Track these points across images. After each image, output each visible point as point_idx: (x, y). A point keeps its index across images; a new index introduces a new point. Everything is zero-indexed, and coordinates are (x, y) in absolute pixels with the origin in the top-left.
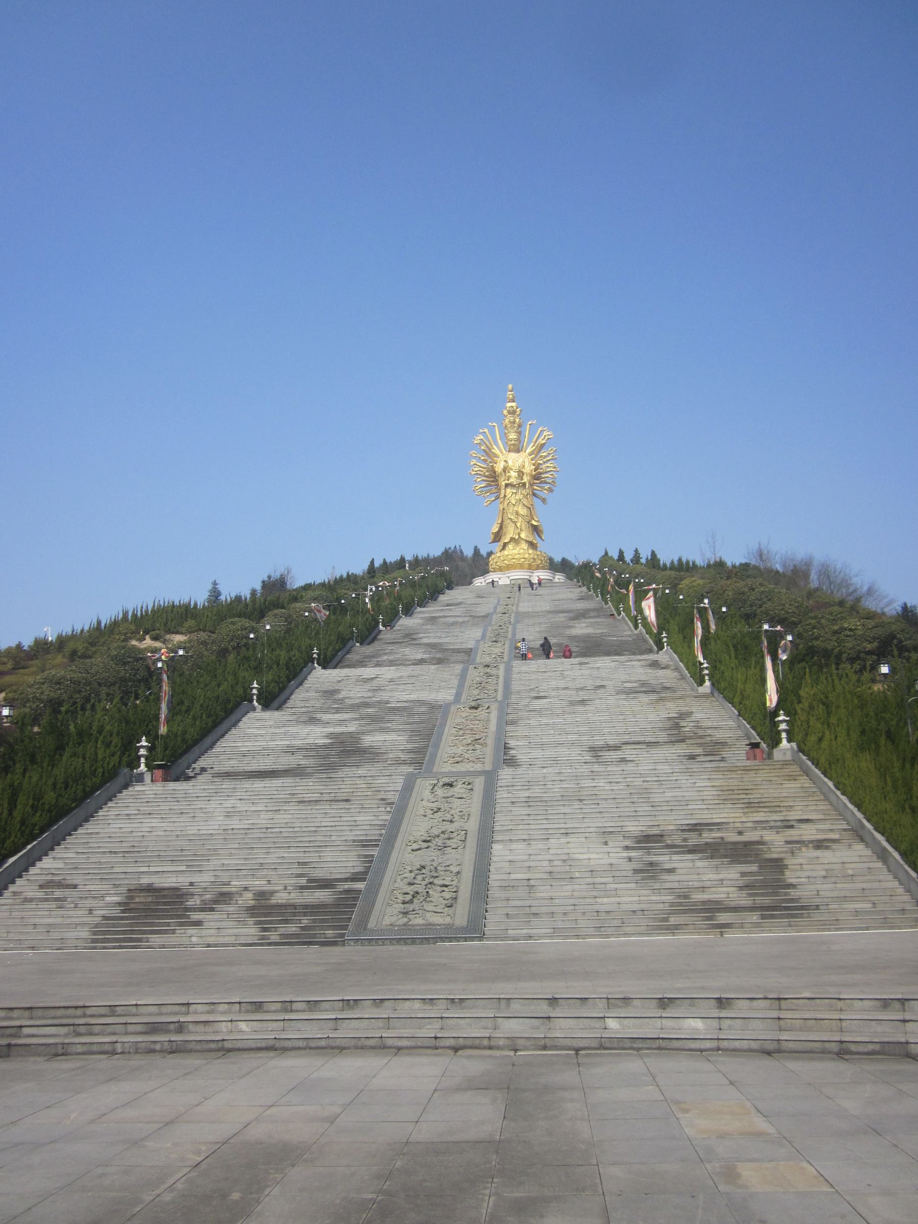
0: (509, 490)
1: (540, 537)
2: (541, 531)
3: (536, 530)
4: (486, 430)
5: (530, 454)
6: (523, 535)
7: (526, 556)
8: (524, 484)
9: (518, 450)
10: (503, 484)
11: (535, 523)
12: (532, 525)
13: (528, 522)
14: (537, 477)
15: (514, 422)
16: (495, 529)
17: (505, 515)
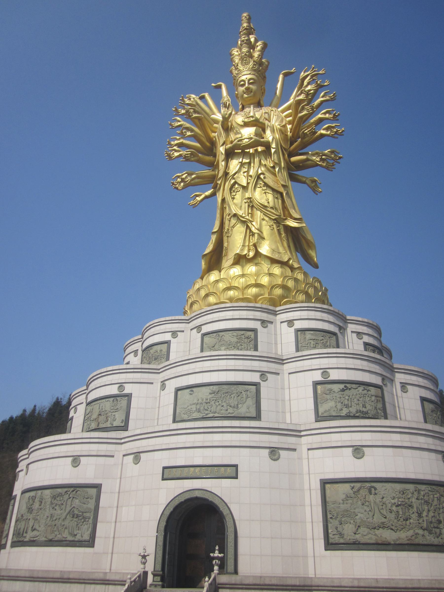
0: (234, 164)
1: (308, 259)
2: (310, 244)
3: (296, 239)
4: (207, 95)
5: (283, 112)
6: (265, 249)
7: (265, 280)
8: (267, 146)
9: (259, 105)
10: (222, 149)
11: (292, 223)
12: (288, 229)
13: (278, 221)
14: (297, 141)
15: (251, 56)
16: (209, 248)
17: (227, 211)
